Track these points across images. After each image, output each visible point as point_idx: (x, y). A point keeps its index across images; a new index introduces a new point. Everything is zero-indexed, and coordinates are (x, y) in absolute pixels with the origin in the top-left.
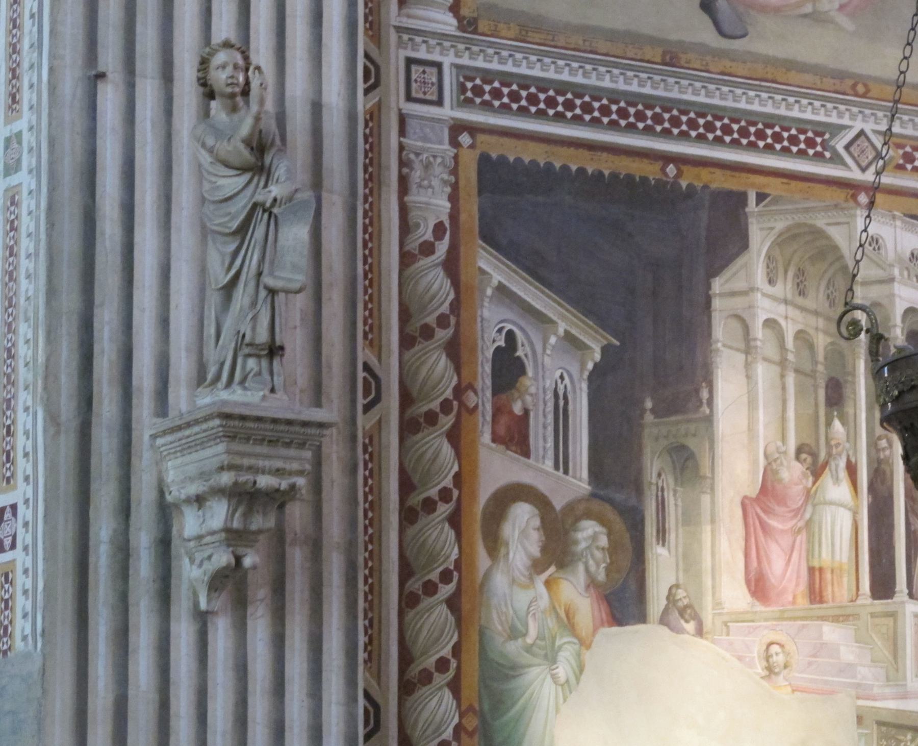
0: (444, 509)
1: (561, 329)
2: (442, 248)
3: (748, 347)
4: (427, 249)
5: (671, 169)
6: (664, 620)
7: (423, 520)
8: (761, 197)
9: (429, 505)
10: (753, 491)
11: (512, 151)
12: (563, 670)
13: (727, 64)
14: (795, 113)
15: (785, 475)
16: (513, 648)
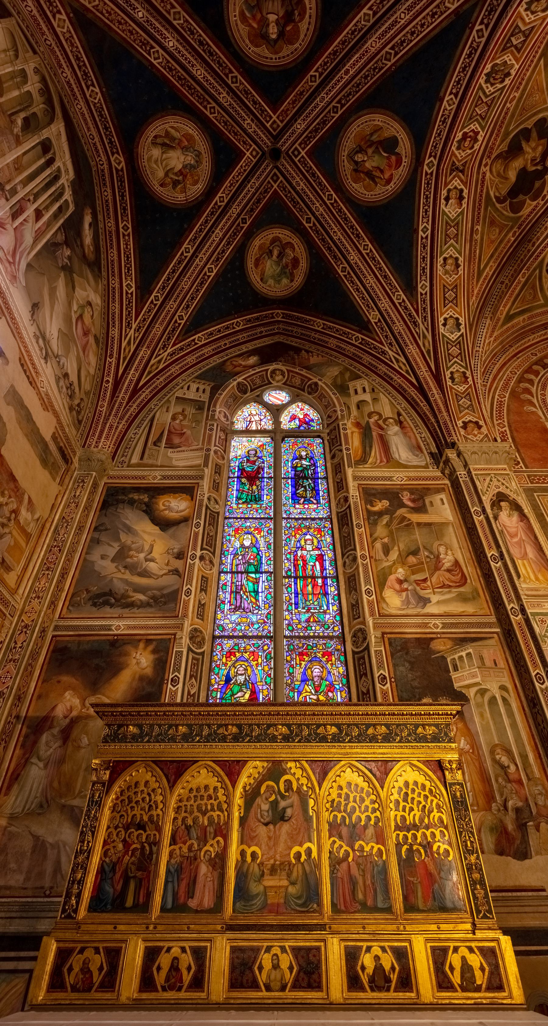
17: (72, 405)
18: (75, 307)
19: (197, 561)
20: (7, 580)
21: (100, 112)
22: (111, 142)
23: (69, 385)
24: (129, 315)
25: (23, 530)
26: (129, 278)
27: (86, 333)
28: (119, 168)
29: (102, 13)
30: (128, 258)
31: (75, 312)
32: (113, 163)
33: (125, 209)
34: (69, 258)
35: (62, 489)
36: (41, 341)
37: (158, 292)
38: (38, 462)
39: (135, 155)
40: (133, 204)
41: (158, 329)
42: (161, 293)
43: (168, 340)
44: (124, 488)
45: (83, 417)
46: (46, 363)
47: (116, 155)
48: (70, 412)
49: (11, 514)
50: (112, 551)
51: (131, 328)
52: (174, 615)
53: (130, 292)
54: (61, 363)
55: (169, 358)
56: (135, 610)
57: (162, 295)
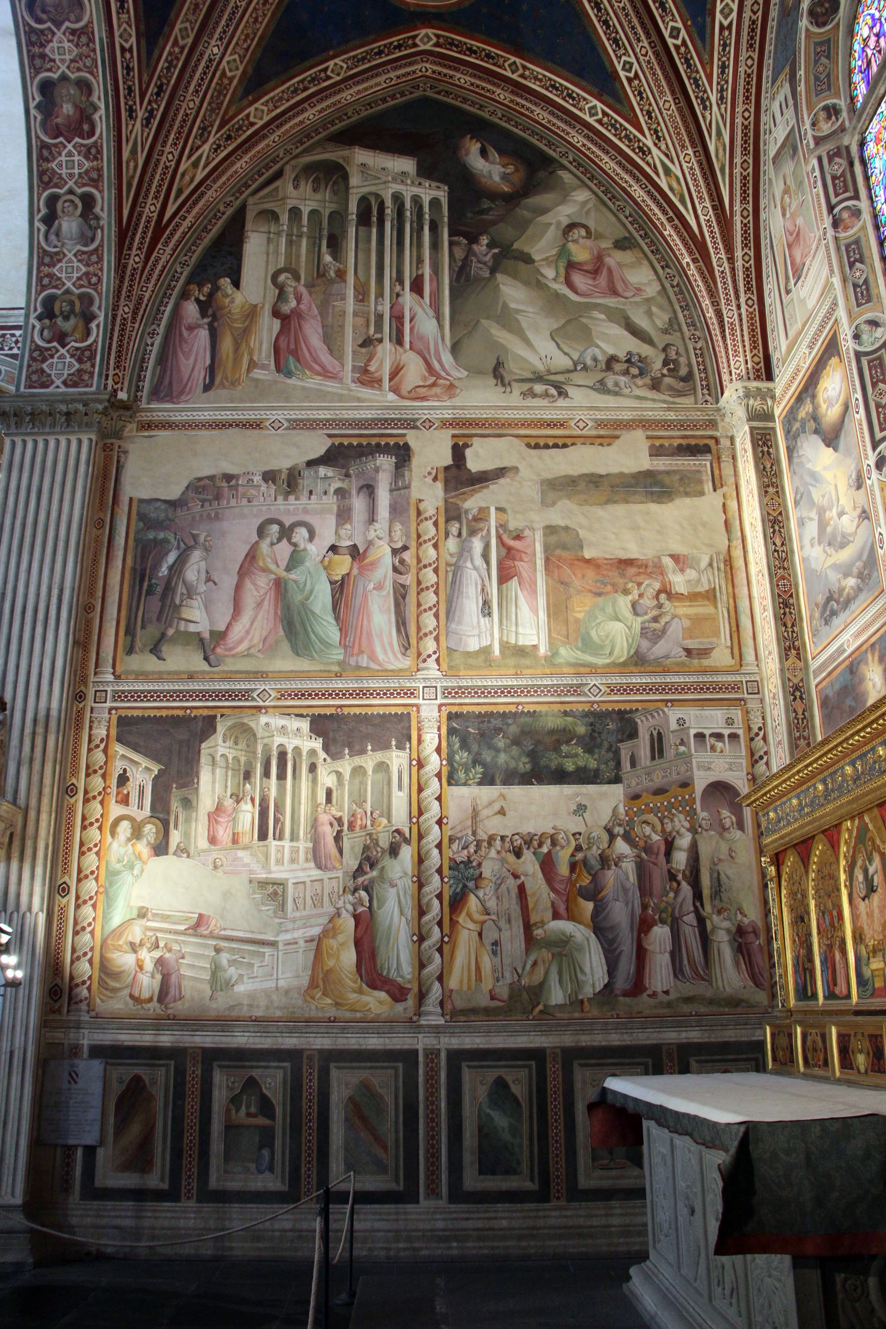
0: (97, 825)
1: (144, 765)
2: (102, 746)
3: (214, 763)
4: (97, 746)
5: (188, 711)
6: (175, 854)
7: (89, 828)
8: (222, 716)
9: (91, 824)
10: (213, 810)
11: (130, 713)
12: (136, 872)
13: (212, 676)
14: (238, 687)
15: (226, 804)
16: (118, 866)
17: (653, 379)
18: (549, 273)
19: (875, 474)
20: (713, 664)
21: (358, 61)
22: (399, 47)
23: (626, 365)
24: (630, 141)
25: (693, 597)
26: (582, 103)
27: (596, 268)
28: (435, 40)
29: (247, 50)
30: (553, 87)
31: (555, 279)
32: (428, 47)
33: (489, 56)
34: (490, 246)
35: (729, 490)
36: (539, 388)
37: (619, 58)
38: (653, 507)
39: (418, 10)
40: (483, 37)
41: (667, 105)
42: (622, 51)
43: (698, 86)
44: (792, 408)
45: (690, 365)
46: (567, 395)
47: (417, 41)
48: (659, 391)
49: (657, 599)
50: (812, 529)
51: (650, 153)
52: (879, 590)
53: (600, 116)
54: (589, 362)
55: (723, 107)
56: (853, 607)
57: (626, 53)
